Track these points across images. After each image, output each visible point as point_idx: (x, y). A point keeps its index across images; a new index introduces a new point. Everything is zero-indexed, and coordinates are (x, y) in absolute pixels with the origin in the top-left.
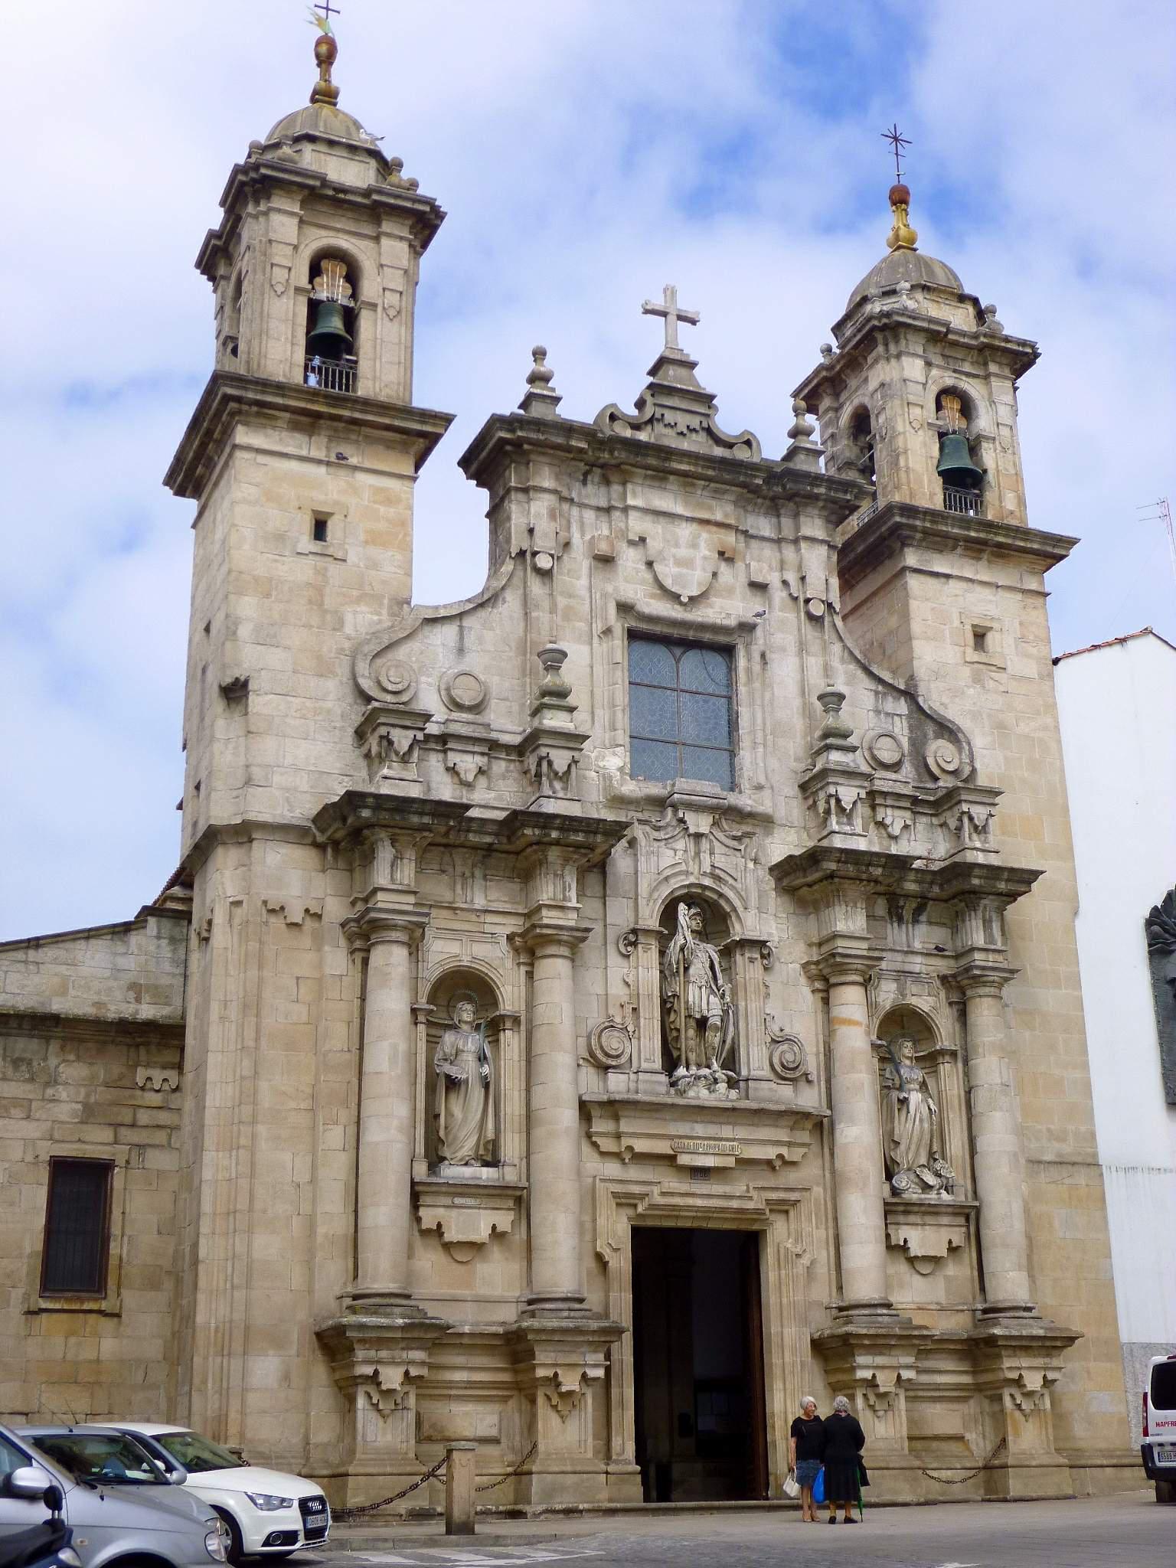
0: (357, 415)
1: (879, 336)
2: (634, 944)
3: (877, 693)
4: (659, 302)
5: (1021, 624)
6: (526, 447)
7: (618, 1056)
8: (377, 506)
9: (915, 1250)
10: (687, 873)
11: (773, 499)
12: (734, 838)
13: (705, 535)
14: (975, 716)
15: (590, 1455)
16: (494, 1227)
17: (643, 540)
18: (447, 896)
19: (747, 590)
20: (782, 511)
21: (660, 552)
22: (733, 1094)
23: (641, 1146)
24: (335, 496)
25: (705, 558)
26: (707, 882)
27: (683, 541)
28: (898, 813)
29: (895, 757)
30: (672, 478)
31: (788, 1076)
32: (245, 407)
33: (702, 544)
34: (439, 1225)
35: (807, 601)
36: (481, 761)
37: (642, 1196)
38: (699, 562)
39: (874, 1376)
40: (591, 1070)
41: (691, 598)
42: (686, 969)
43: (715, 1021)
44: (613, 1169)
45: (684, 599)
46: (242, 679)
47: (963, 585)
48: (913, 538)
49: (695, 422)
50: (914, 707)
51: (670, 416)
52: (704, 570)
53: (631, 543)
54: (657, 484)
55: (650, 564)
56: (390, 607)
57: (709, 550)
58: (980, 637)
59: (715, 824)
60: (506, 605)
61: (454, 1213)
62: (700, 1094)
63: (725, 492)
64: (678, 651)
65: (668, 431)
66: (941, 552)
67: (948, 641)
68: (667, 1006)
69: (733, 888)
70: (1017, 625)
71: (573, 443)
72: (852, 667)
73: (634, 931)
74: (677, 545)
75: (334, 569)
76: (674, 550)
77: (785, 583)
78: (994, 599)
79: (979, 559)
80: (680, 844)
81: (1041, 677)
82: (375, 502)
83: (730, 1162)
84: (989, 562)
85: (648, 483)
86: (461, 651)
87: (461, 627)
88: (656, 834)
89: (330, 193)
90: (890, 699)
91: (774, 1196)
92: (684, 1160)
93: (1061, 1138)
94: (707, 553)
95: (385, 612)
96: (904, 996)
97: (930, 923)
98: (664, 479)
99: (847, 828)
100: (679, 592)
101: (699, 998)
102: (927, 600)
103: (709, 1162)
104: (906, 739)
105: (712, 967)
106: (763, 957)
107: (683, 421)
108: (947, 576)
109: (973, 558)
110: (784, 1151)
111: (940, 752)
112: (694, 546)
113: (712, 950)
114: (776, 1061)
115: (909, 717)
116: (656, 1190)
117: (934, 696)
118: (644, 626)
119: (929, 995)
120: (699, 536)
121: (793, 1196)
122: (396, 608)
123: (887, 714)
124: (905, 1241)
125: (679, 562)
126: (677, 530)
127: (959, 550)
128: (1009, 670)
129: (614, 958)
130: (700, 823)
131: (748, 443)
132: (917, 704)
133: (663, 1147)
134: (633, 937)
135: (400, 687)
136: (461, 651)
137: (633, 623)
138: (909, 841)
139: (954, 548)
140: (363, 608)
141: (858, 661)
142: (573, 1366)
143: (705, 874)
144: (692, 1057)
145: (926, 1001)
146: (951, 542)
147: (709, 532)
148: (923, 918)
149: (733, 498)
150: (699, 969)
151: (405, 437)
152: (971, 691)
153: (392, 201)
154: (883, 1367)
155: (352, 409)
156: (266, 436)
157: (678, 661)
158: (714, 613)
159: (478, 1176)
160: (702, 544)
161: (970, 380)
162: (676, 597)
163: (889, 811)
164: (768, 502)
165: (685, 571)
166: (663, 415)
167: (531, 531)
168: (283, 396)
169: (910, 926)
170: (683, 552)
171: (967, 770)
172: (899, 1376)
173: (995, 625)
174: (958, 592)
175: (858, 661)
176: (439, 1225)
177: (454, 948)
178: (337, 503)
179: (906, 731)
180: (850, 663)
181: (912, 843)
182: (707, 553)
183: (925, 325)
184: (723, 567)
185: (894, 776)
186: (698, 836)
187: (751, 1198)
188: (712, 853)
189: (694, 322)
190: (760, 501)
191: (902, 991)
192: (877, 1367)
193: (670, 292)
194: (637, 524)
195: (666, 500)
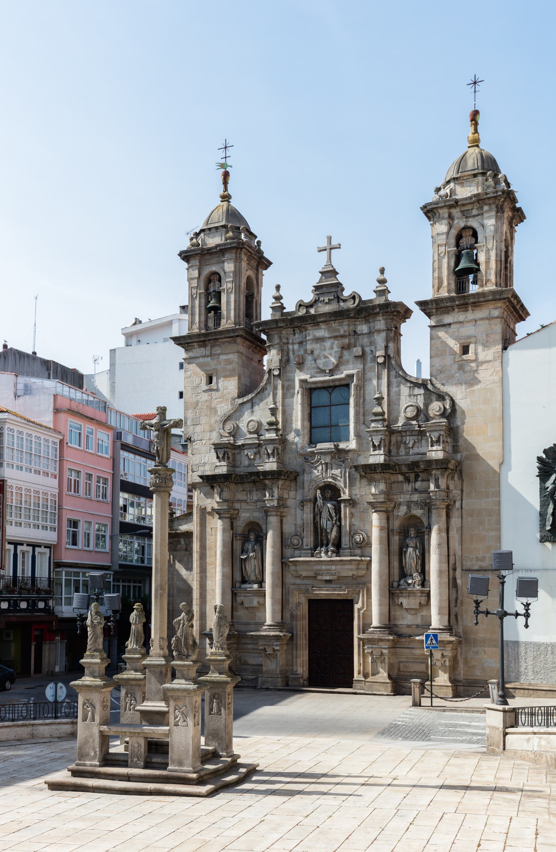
0: (214, 337)
2: (303, 506)
3: (410, 387)
4: (324, 244)
5: (487, 335)
9: (405, 605)
11: (365, 317)
12: (341, 461)
13: (336, 342)
15: (278, 672)
17: (312, 352)
18: (245, 498)
20: (370, 321)
21: (319, 355)
23: (304, 574)
24: (214, 367)
25: (336, 352)
26: (330, 480)
27: (327, 348)
28: (412, 438)
33: (335, 346)
36: (255, 450)
38: (333, 354)
39: (372, 652)
40: (292, 550)
41: (330, 370)
43: (329, 531)
44: (298, 581)
45: (327, 371)
47: (458, 325)
48: (432, 312)
53: (309, 354)
54: (317, 327)
55: (315, 360)
56: (231, 402)
59: (332, 458)
61: (246, 599)
63: (343, 322)
64: (330, 390)
66: (448, 313)
70: (484, 336)
71: (279, 325)
73: (302, 502)
74: (325, 350)
79: (467, 311)
84: (473, 310)
85: (314, 328)
89: (206, 252)
90: (416, 388)
92: (319, 577)
93: (483, 559)
94: (337, 349)
95: (229, 404)
96: (410, 511)
97: (422, 480)
98: (318, 325)
101: (325, 523)
103: (328, 578)
106: (350, 504)
108: (450, 324)
110: (355, 573)
111: (435, 407)
112: (332, 348)
114: (353, 541)
115: (424, 394)
118: (313, 386)
120: (334, 343)
123: (414, 395)
124: (401, 603)
126: (325, 344)
127: (456, 310)
129: (299, 512)
131: (354, 298)
133: (311, 574)
134: (302, 503)
137: (309, 386)
138: (418, 448)
139: (454, 310)
142: (269, 645)
144: (325, 542)
145: (418, 512)
146: (450, 308)
147: (338, 340)
148: (420, 479)
149: (347, 323)
153: (224, 247)
155: (212, 336)
156: (193, 352)
157: (330, 394)
160: (335, 346)
163: (408, 438)
168: (191, 339)
172: (382, 652)
176: (242, 602)
177: (248, 515)
178: (214, 369)
179: (423, 401)
181: (420, 448)
182: (337, 349)
183: (443, 204)
184: (346, 353)
190: (360, 320)
191: (409, 508)
193: (330, 239)
194: (309, 347)
195: (322, 332)
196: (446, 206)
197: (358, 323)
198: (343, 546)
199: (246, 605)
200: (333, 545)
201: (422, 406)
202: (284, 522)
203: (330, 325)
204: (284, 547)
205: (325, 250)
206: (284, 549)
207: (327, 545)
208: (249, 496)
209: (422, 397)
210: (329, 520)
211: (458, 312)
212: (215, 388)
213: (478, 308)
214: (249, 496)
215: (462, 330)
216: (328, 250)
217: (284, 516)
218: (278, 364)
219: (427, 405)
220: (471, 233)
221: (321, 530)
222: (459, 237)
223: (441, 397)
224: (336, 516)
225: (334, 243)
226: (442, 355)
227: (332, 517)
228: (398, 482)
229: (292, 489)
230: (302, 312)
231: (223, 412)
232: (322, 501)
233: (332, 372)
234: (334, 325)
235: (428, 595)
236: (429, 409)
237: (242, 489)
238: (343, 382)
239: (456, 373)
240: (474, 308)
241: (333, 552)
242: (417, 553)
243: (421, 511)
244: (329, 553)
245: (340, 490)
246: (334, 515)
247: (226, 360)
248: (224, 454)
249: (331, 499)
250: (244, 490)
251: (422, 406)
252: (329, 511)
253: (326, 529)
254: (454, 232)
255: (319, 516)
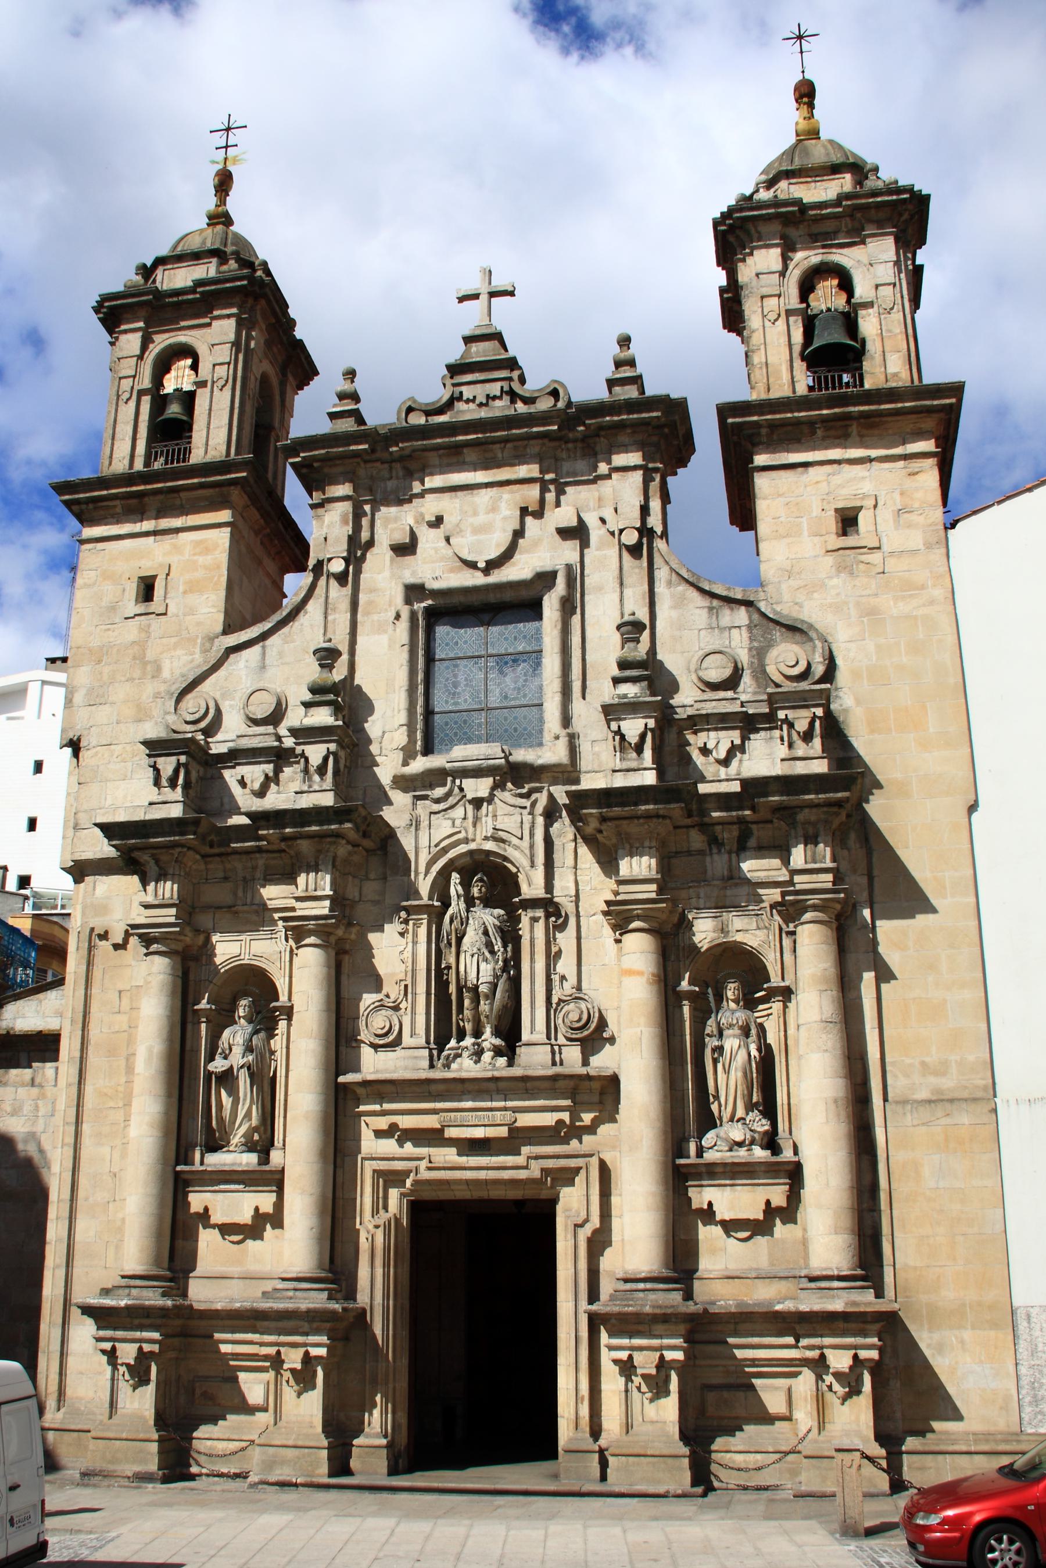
1: (731, 239)
4: (475, 283)
5: (902, 494)
6: (316, 465)
7: (386, 1034)
8: (196, 558)
10: (466, 841)
12: (521, 796)
14: (837, 608)
16: (257, 1209)
19: (557, 537)
22: (502, 1061)
25: (505, 518)
26: (490, 846)
29: (727, 672)
30: (465, 451)
31: (574, 1036)
32: (84, 507)
34: (206, 1209)
35: (621, 531)
37: (407, 1173)
39: (630, 1357)
42: (459, 940)
43: (483, 989)
46: (75, 739)
47: (828, 468)
49: (495, 389)
50: (756, 616)
51: (467, 392)
52: (504, 531)
54: (454, 460)
55: (448, 540)
56: (203, 645)
57: (510, 509)
58: (848, 521)
60: (307, 616)
62: (465, 1067)
63: (525, 447)
65: (472, 406)
67: (806, 533)
68: (439, 977)
69: (516, 847)
70: (897, 496)
72: (682, 587)
74: (475, 514)
75: (155, 622)
76: (471, 520)
77: (603, 521)
78: (867, 474)
80: (458, 812)
81: (929, 546)
82: (194, 555)
83: (503, 1132)
84: (861, 436)
86: (263, 667)
87: (264, 647)
88: (436, 807)
91: (550, 1164)
92: (452, 1133)
94: (508, 513)
95: (198, 650)
99: (634, 764)
100: (474, 559)
102: (780, 496)
103: (479, 1133)
104: (746, 651)
105: (486, 933)
107: (480, 392)
109: (838, 437)
112: (494, 509)
113: (488, 917)
114: (560, 1021)
115: (750, 627)
116: (423, 1164)
117: (786, 597)
119: (758, 928)
121: (573, 1163)
122: (208, 645)
125: (477, 530)
127: (820, 433)
128: (885, 548)
130: (480, 787)
131: (555, 393)
132: (759, 610)
133: (430, 1122)
135: (202, 711)
136: (263, 667)
140: (179, 652)
141: (687, 581)
143: (486, 838)
144: (469, 1027)
147: (512, 492)
148: (752, 842)
150: (472, 938)
151: (217, 490)
152: (835, 581)
154: (641, 1349)
158: (519, 570)
159: (238, 1161)
160: (503, 505)
161: (845, 251)
162: (472, 565)
164: (579, 445)
165: (482, 537)
166: (461, 393)
167: (326, 539)
169: (734, 856)
170: (482, 518)
171: (819, 670)
173: (865, 503)
174: (819, 478)
175: (687, 581)
176: (206, 1209)
179: (746, 642)
180: (679, 584)
185: (730, 694)
186: (477, 803)
187: (526, 1168)
188: (495, 816)
189: (512, 294)
190: (570, 445)
192: (633, 1348)
196: (778, 216)
197: (564, 455)
198: (526, 1036)
199: (216, 1218)
200: (497, 1033)
201: (744, 657)
202: (345, 969)
203: (489, 455)
204: (343, 1041)
205: (476, 296)
206: (342, 1049)
207: (477, 1034)
208: (240, 894)
209: (745, 634)
210: (486, 960)
211: (824, 438)
212: (162, 610)
213: (876, 432)
214: (240, 894)
215: (837, 480)
216: (484, 297)
217: (346, 952)
218: (345, 547)
219: (759, 654)
220: (835, 282)
221: (460, 989)
222: (806, 288)
223: (795, 630)
224: (505, 946)
225: (500, 282)
226: (787, 536)
227: (493, 952)
228: (689, 853)
229: (372, 876)
230: (418, 420)
231: (177, 672)
232: (463, 906)
233: (492, 565)
234: (500, 455)
235: (794, 1174)
236: (767, 661)
237: (221, 875)
238: (525, 594)
239: (830, 578)
240: (864, 432)
241: (498, 1052)
242: (754, 1052)
243: (761, 934)
244: (487, 1056)
245: (515, 877)
246: (498, 946)
247: (198, 543)
248: (176, 772)
249: (488, 902)
250: (226, 879)
251: (744, 657)
252: (486, 933)
253: (477, 987)
254: (794, 275)
255: (453, 949)
